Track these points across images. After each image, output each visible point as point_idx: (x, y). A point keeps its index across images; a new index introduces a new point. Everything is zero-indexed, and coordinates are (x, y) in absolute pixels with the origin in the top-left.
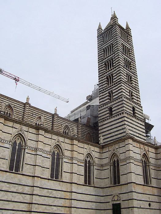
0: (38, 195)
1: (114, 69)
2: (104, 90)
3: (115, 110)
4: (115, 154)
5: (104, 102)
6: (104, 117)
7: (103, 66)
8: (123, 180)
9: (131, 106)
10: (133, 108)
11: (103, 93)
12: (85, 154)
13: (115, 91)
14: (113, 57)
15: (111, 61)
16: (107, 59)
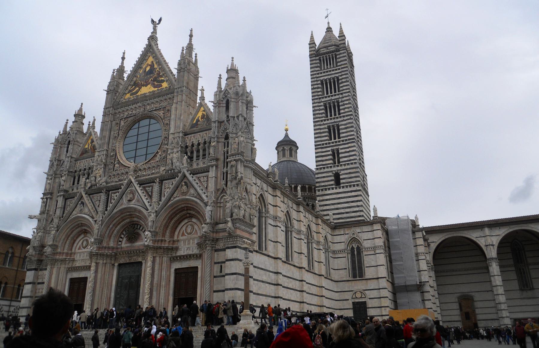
0: (305, 291)
1: (342, 119)
2: (323, 144)
3: (344, 179)
4: (354, 239)
5: (324, 163)
6: (326, 184)
7: (321, 108)
8: (369, 273)
9: (362, 174)
10: (363, 178)
11: (322, 148)
12: (324, 236)
13: (343, 151)
14: (340, 100)
15: (336, 104)
16: (328, 99)
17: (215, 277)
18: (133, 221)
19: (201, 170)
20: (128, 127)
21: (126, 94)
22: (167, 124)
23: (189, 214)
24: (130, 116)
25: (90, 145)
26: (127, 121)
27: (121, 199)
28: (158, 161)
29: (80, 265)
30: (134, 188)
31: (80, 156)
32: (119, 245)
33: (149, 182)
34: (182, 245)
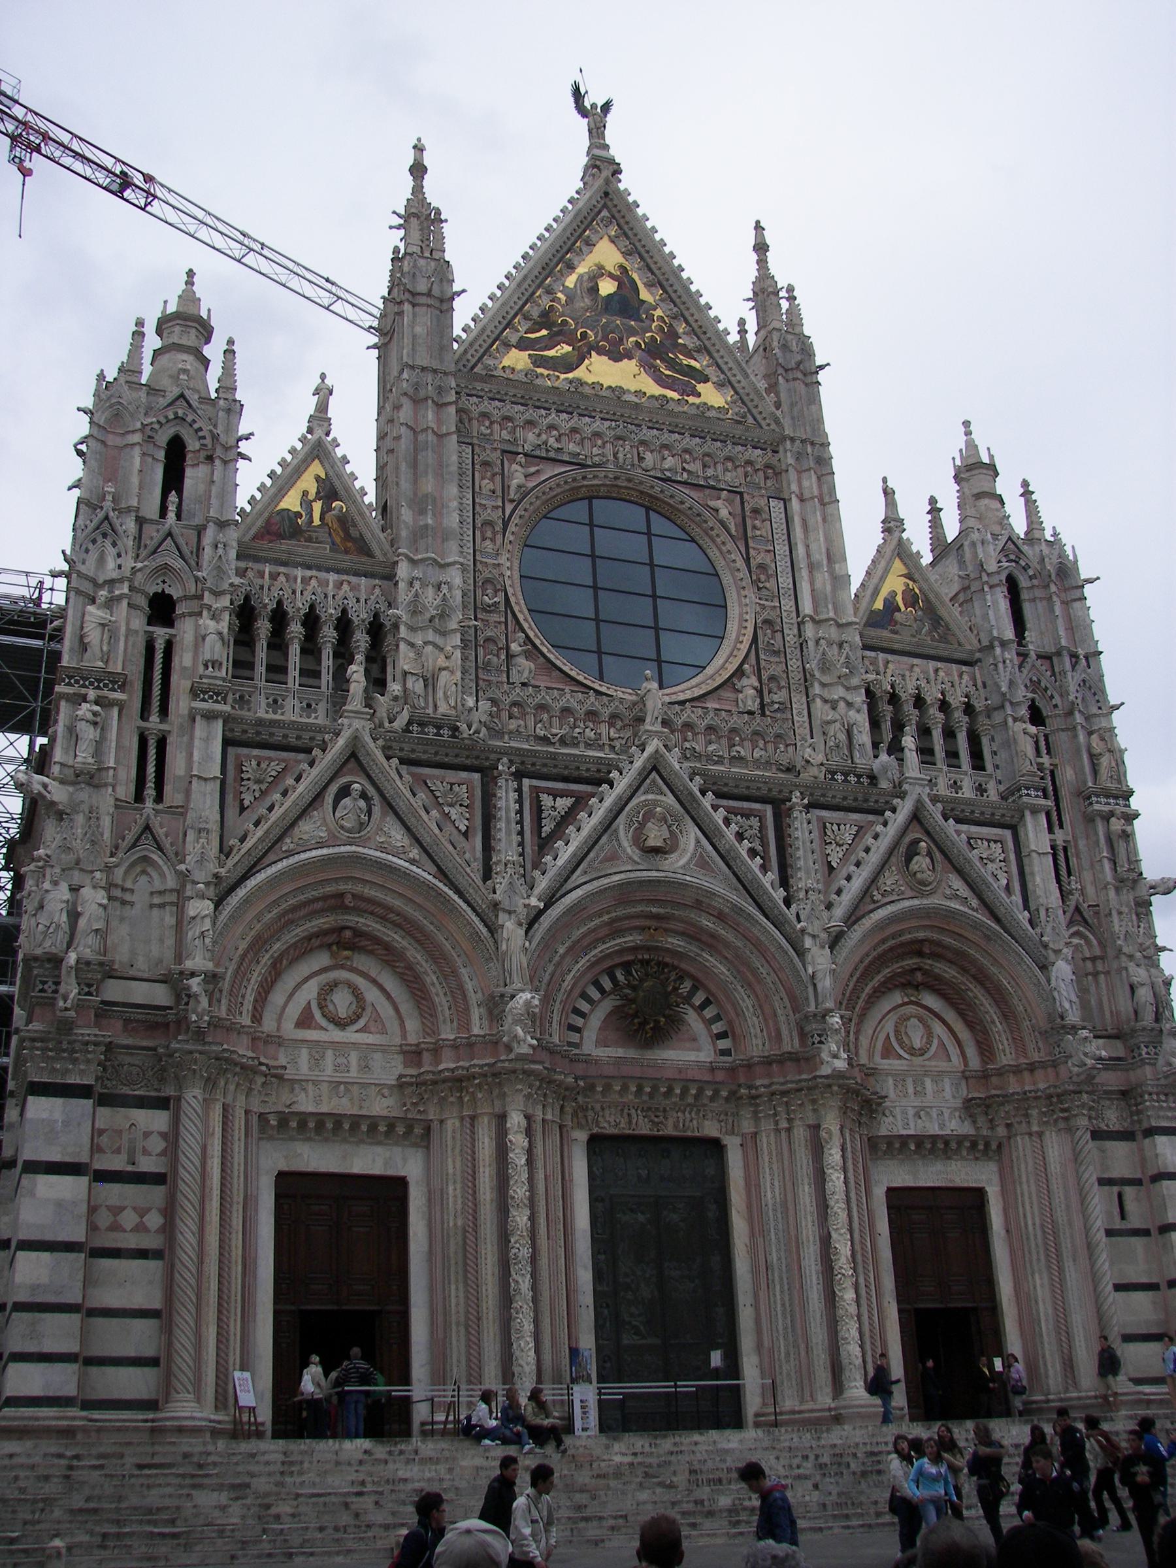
17: (1110, 1233)
18: (648, 949)
19: (982, 813)
20: (543, 504)
21: (507, 346)
22: (762, 567)
23: (926, 973)
24: (552, 454)
25: (317, 507)
26: (538, 471)
27: (605, 831)
28: (750, 713)
29: (324, 1109)
30: (670, 799)
31: (255, 538)
32: (570, 1044)
33: (746, 792)
34: (892, 1095)
